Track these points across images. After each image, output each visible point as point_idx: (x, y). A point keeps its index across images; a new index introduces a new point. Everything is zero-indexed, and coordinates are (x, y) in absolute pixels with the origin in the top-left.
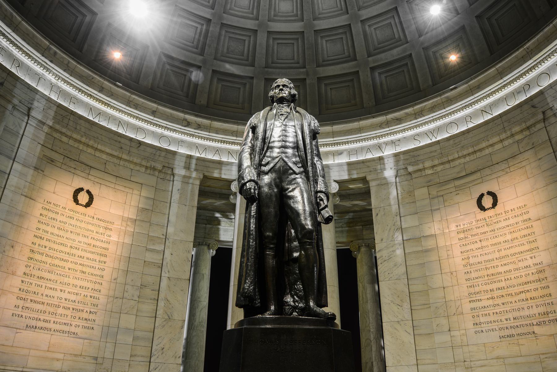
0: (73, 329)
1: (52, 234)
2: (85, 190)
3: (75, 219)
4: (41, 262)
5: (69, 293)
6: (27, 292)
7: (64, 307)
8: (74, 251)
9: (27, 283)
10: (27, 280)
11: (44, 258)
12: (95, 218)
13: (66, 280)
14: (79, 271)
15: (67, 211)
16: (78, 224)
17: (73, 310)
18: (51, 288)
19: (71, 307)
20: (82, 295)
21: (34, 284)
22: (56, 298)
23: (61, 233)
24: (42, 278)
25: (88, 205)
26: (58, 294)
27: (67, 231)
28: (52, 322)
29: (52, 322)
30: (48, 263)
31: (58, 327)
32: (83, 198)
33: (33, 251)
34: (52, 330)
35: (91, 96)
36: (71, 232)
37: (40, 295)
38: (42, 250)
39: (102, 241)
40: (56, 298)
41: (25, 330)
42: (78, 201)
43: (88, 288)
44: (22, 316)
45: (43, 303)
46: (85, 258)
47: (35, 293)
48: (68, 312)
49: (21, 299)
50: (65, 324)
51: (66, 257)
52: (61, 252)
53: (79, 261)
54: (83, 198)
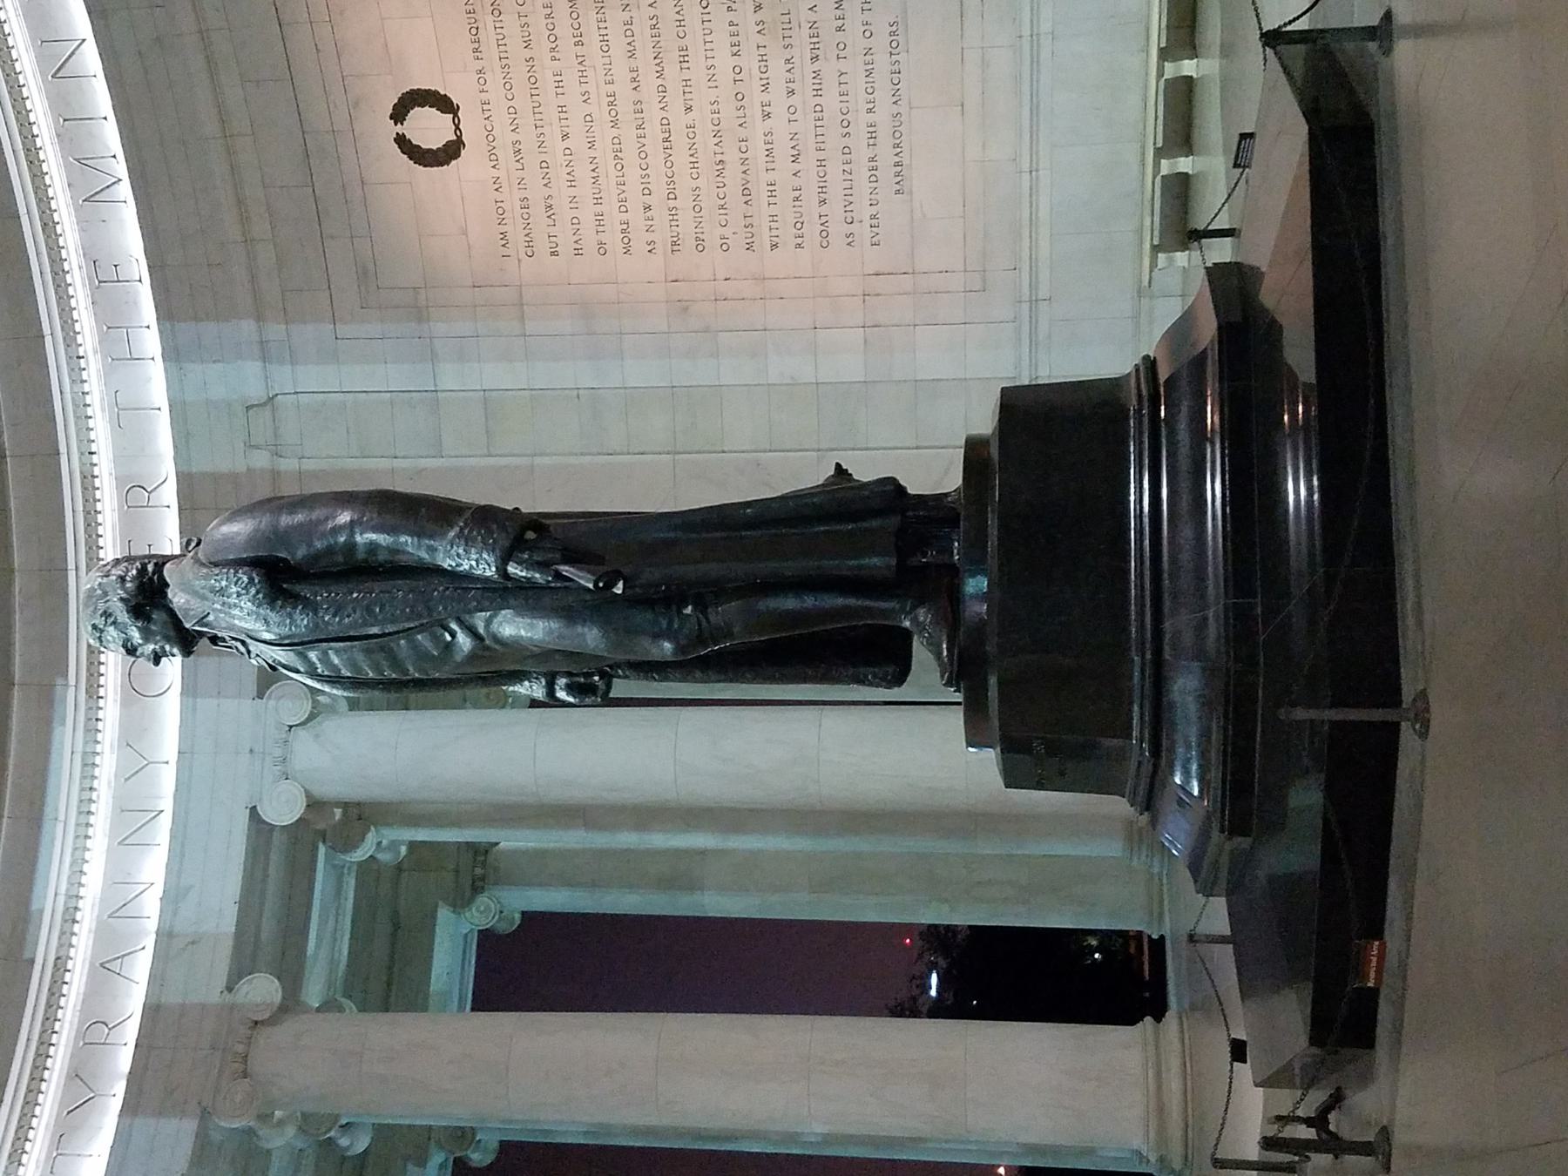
0: (881, 41)
1: (598, 201)
2: (399, 129)
3: (515, 137)
4: (697, 208)
5: (765, 88)
6: (799, 224)
7: (818, 92)
8: (625, 108)
9: (774, 233)
10: (766, 234)
11: (684, 202)
12: (478, 65)
13: (728, 111)
14: (686, 75)
15: (502, 174)
16: (526, 121)
17: (815, 58)
18: (769, 153)
19: (810, 68)
20: (761, 40)
21: (773, 210)
22: (794, 127)
23: (583, 172)
24: (746, 191)
25: (445, 104)
26: (779, 124)
27: (568, 152)
28: (871, 118)
29: (871, 118)
30: (694, 184)
31: (883, 96)
32: (428, 128)
33: (674, 244)
34: (895, 109)
35: (49, 227)
36: (565, 136)
37: (797, 182)
38: (660, 215)
39: (548, 16)
40: (794, 127)
41: (911, 193)
42: (448, 145)
43: (731, 24)
44: (873, 217)
45: (821, 163)
46: (633, 63)
47: (797, 199)
48: (829, 68)
49: (825, 234)
50: (869, 73)
51: (654, 130)
52: (643, 154)
53: (649, 82)
54: (428, 128)
